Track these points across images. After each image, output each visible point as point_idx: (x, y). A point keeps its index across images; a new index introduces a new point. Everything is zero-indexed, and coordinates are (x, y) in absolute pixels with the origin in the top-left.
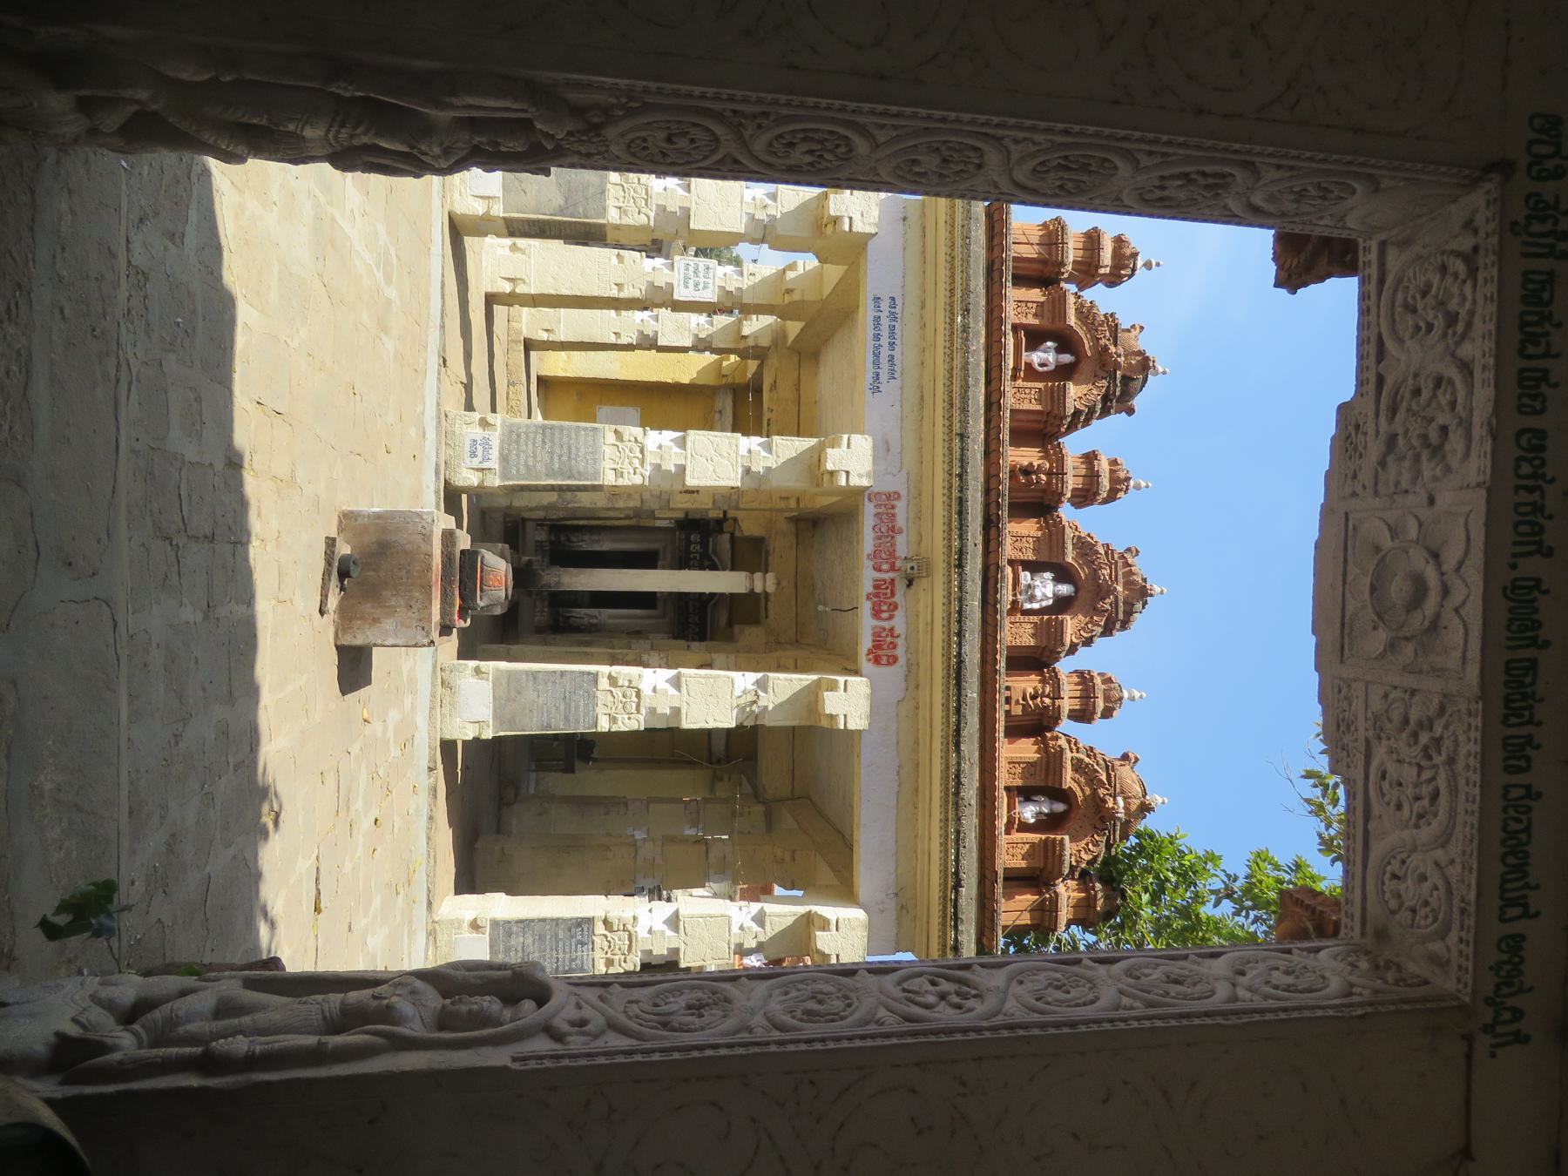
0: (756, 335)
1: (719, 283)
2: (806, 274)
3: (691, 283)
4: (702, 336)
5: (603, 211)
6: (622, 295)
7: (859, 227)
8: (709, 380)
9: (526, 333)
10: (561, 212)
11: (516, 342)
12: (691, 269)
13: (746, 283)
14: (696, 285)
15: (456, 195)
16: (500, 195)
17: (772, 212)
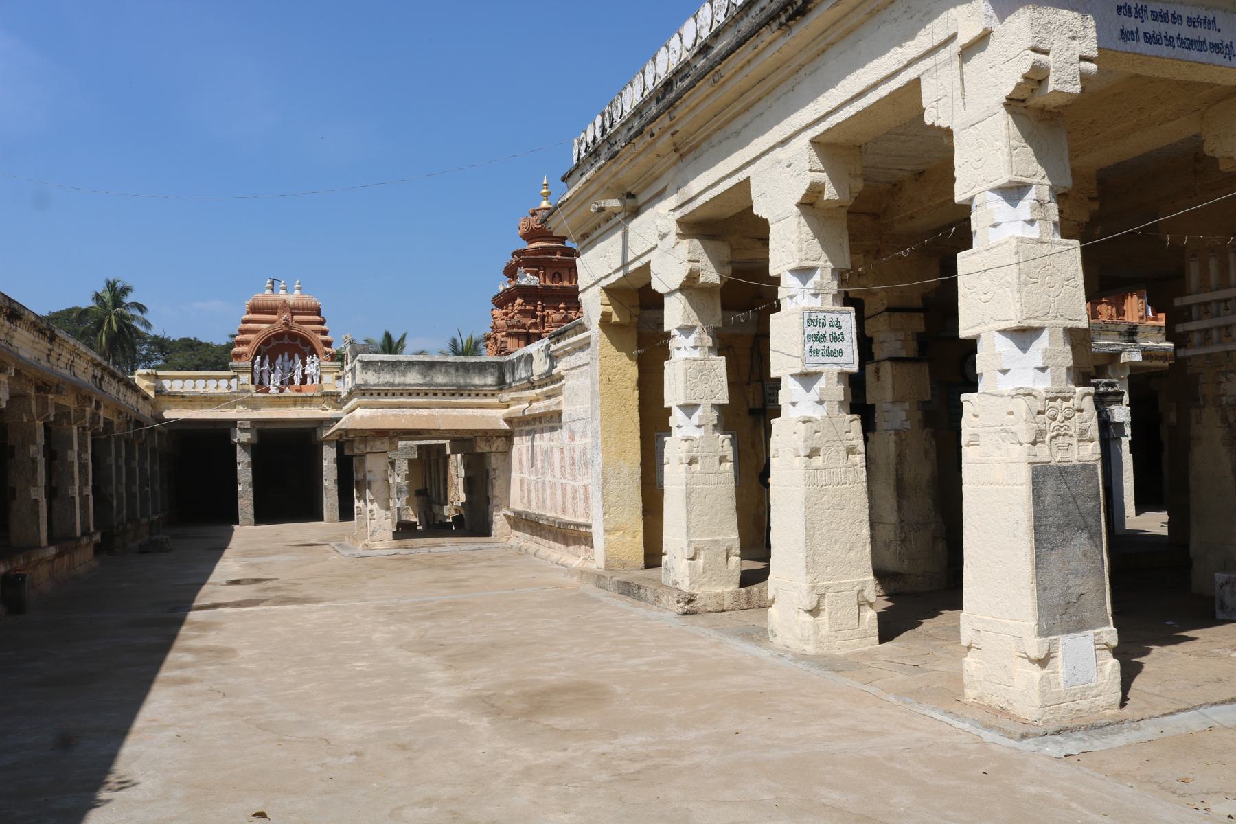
0: (719, 265)
1: (829, 303)
2: (829, 169)
3: (835, 346)
4: (709, 341)
5: (1085, 467)
6: (861, 448)
7: (1090, 46)
8: (632, 338)
9: (733, 587)
10: (1094, 536)
11: (749, 602)
12: (817, 345)
13: (824, 265)
14: (837, 338)
15: (1101, 701)
16: (1091, 633)
17: (1046, 194)
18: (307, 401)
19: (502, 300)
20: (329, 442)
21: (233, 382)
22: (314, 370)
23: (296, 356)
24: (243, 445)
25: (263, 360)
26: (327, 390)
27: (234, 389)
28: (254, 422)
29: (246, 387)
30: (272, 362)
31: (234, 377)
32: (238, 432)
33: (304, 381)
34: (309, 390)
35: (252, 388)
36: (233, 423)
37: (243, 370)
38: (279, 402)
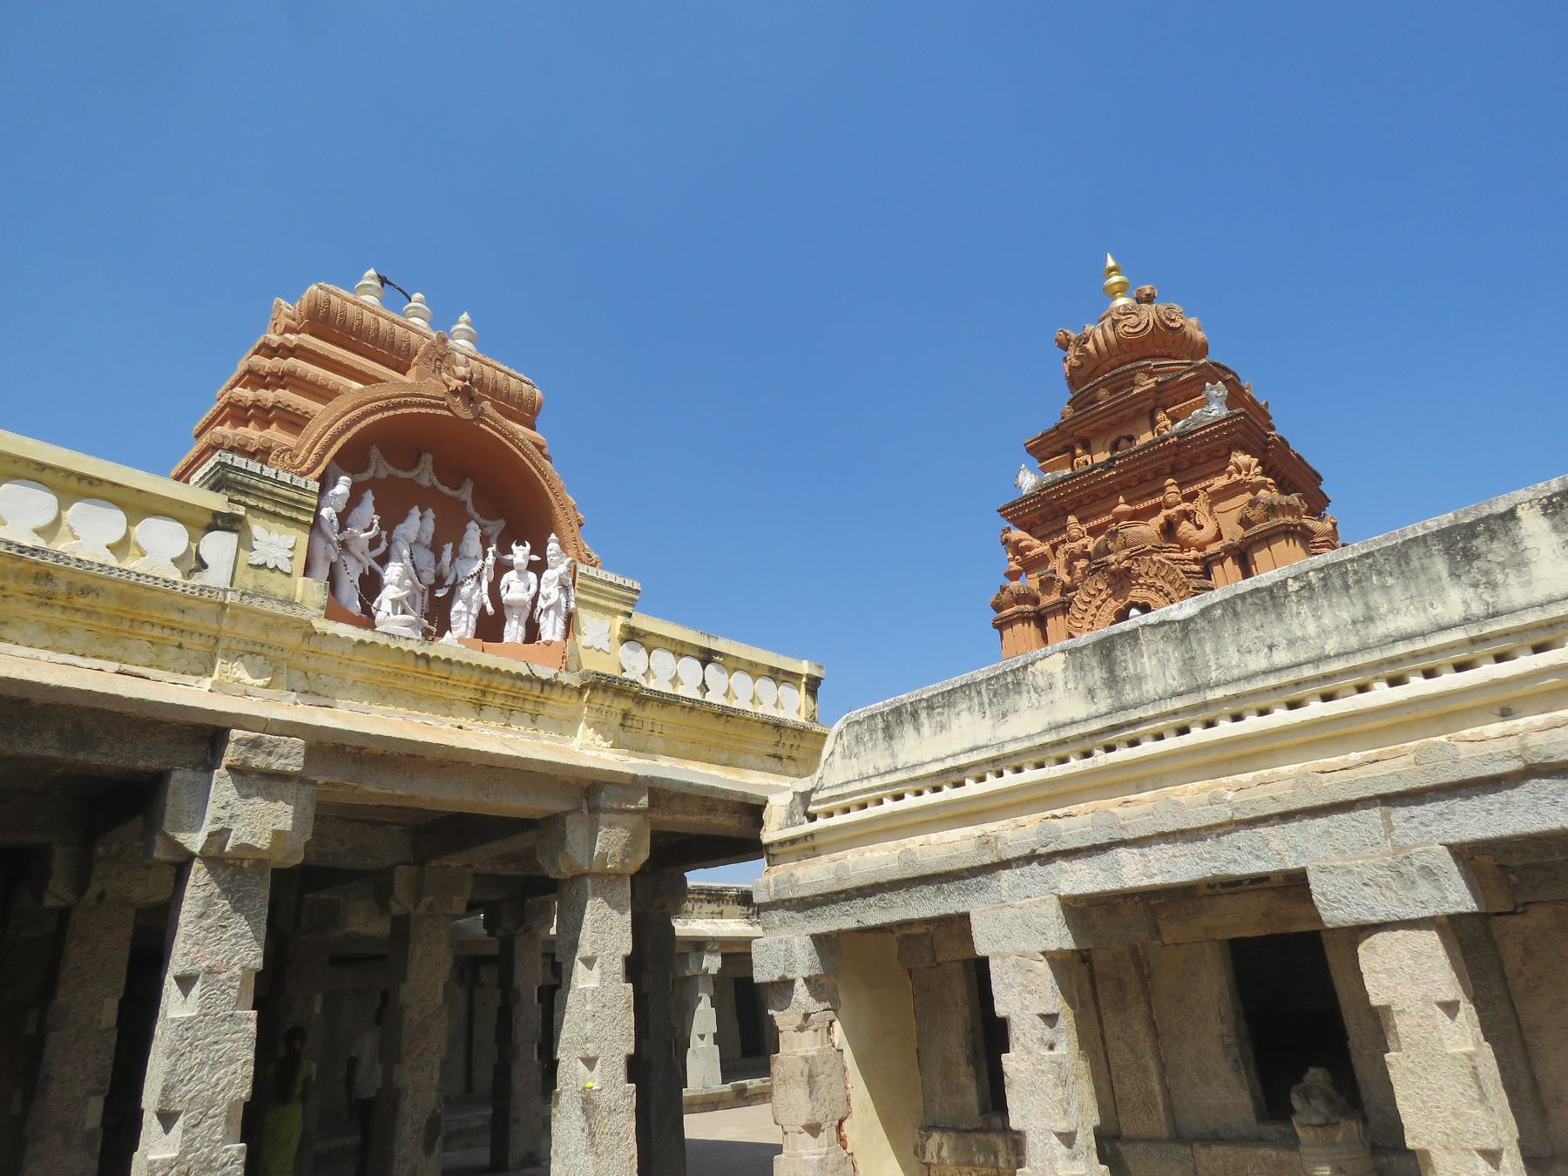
18: (525, 696)
19: (1041, 514)
20: (606, 880)
21: (218, 546)
22: (551, 591)
23: (473, 533)
24: (229, 865)
25: (354, 500)
26: (594, 664)
27: (216, 576)
28: (328, 748)
29: (274, 584)
30: (391, 518)
31: (228, 523)
32: (222, 787)
33: (489, 628)
34: (510, 653)
35: (310, 593)
36: (204, 737)
37: (284, 509)
38: (419, 679)
